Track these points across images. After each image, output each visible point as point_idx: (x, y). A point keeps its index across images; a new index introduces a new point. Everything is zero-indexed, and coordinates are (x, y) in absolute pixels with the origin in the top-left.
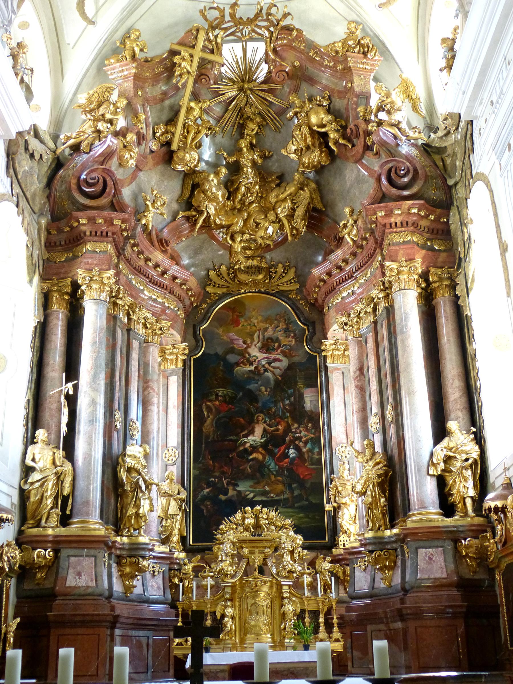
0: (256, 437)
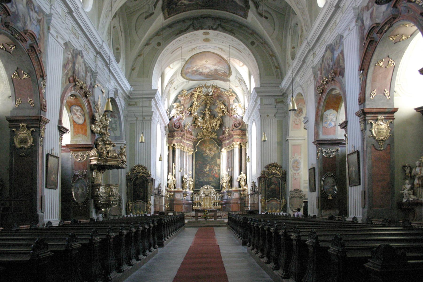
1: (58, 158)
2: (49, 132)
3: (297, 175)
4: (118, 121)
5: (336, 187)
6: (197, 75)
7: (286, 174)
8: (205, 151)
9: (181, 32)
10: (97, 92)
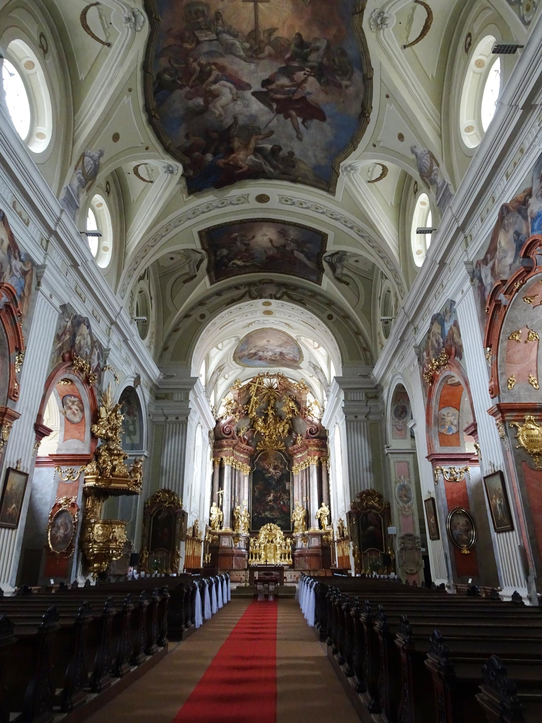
3: (407, 510)
4: (137, 421)
6: (256, 359)
8: (267, 470)
9: (233, 301)
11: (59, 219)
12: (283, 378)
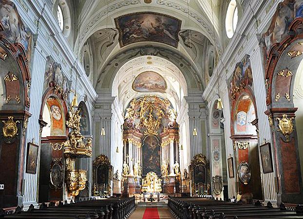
0: (151, 159)
1: (38, 146)
2: (31, 125)
5: (250, 174)
7: (209, 163)
9: (132, 57)
10: (72, 97)
11: (43, 9)
12: (157, 98)
